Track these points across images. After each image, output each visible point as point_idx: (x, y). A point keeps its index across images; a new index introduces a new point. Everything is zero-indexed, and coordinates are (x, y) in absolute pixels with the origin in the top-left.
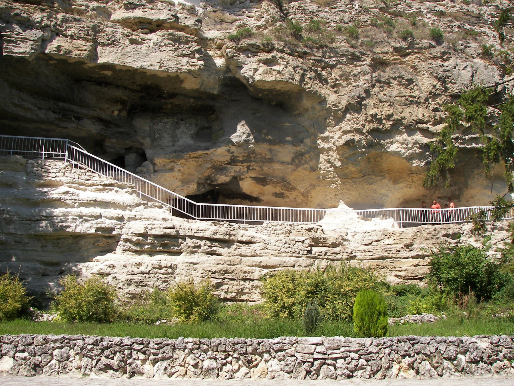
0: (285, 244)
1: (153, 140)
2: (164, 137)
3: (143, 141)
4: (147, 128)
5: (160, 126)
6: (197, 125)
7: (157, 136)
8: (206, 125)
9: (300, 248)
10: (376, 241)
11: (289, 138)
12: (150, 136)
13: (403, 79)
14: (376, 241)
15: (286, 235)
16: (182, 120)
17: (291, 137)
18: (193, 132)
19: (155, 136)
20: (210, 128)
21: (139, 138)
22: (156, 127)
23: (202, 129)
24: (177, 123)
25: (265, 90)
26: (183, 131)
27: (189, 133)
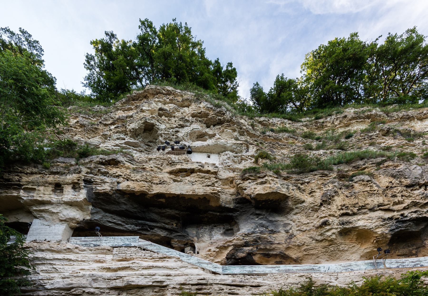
1: (198, 238)
2: (204, 236)
3: (193, 239)
4: (195, 232)
5: (202, 231)
6: (224, 228)
7: (201, 236)
8: (229, 228)
12: (196, 236)
16: (215, 226)
18: (221, 232)
19: (199, 236)
20: (232, 229)
21: (190, 238)
22: (200, 231)
23: (228, 230)
24: (212, 228)
26: (216, 232)
27: (220, 232)
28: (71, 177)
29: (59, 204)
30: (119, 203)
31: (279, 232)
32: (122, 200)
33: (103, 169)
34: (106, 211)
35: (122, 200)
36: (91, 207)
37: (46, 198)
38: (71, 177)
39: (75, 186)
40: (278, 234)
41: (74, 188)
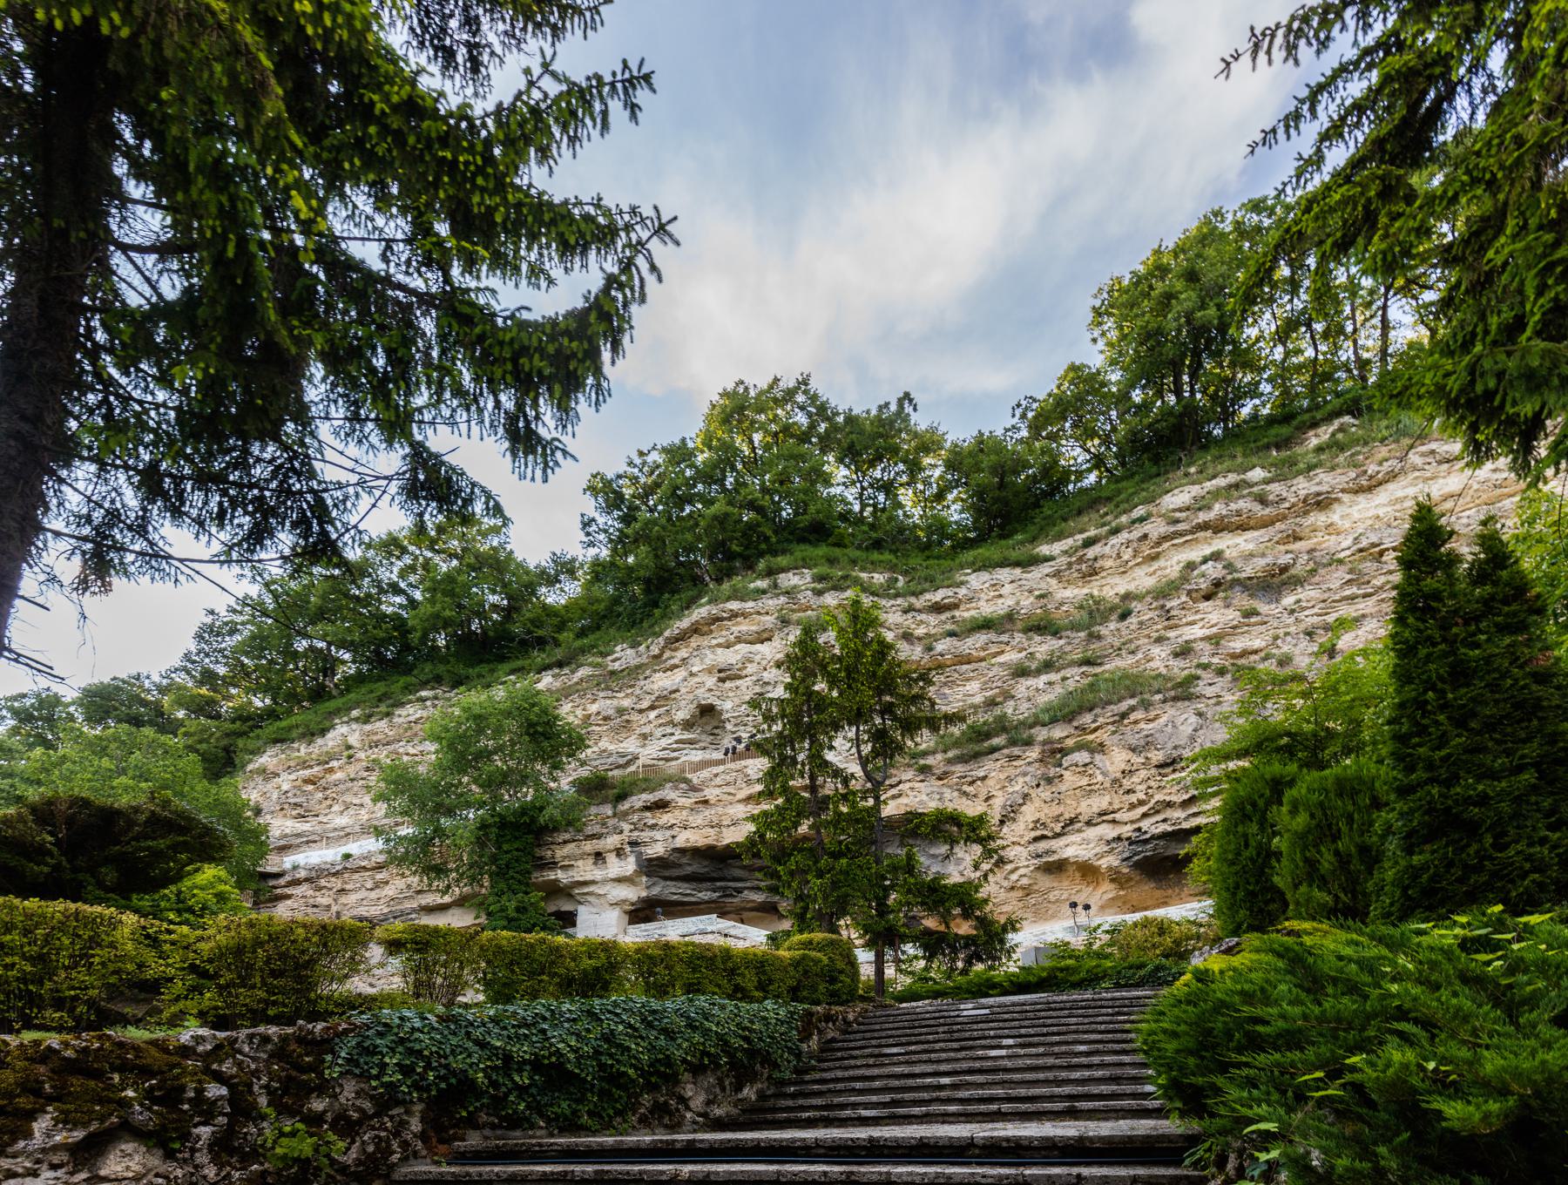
28: (612, 841)
29: (605, 881)
30: (680, 866)
32: (684, 860)
33: (649, 818)
34: (666, 878)
35: (684, 860)
36: (644, 879)
37: (588, 877)
38: (612, 841)
39: (619, 852)
41: (618, 855)
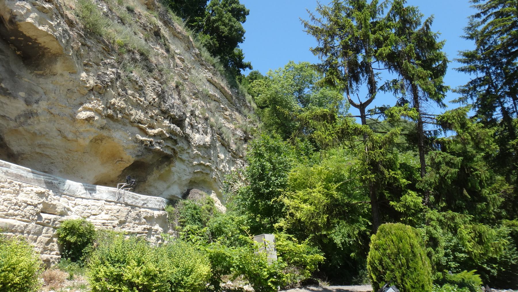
0: (15, 205)
9: (31, 211)
10: (94, 215)
11: (22, 94)
13: (137, 84)
14: (94, 215)
15: (14, 195)
17: (26, 93)
25: (24, 36)
31: (15, 98)
40: (12, 100)
